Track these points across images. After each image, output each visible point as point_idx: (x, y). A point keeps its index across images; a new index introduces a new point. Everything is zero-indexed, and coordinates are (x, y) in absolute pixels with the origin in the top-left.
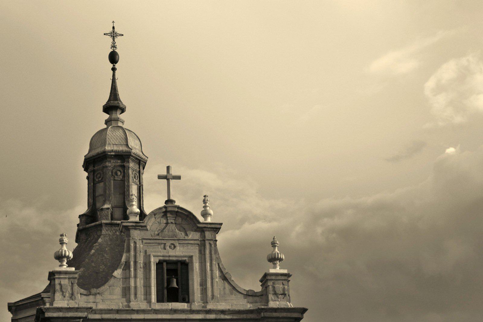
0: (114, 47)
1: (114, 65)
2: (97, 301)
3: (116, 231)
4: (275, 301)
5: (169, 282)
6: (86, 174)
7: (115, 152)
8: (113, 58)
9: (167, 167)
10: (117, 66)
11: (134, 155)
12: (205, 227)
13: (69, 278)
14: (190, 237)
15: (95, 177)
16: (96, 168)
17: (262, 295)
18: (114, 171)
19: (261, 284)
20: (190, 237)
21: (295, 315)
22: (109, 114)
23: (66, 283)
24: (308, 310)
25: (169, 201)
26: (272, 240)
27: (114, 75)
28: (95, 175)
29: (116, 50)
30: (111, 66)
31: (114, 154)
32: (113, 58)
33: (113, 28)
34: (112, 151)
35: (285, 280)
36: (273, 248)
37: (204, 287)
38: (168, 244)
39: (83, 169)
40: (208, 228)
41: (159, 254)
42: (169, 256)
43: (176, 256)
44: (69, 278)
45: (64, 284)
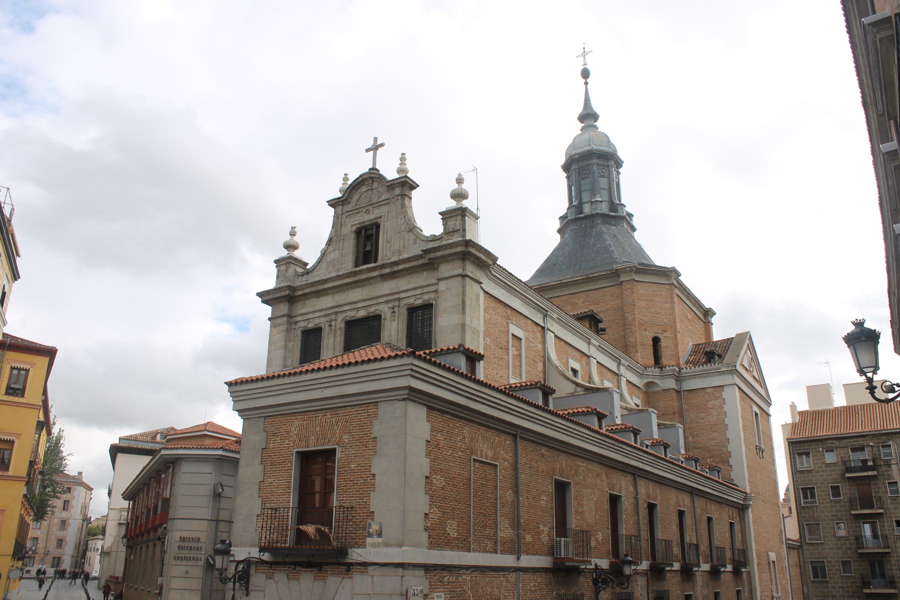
0: (585, 65)
1: (586, 80)
3: (582, 224)
5: (365, 246)
7: (579, 154)
8: (585, 74)
9: (375, 138)
10: (588, 80)
11: (596, 152)
12: (392, 185)
13: (286, 264)
14: (383, 198)
17: (442, 238)
18: (600, 171)
25: (373, 169)
27: (586, 88)
29: (587, 67)
30: (584, 81)
31: (577, 156)
32: (585, 74)
33: (584, 48)
34: (576, 154)
35: (458, 215)
36: (457, 185)
40: (395, 184)
42: (364, 222)
43: (369, 221)
44: (286, 264)
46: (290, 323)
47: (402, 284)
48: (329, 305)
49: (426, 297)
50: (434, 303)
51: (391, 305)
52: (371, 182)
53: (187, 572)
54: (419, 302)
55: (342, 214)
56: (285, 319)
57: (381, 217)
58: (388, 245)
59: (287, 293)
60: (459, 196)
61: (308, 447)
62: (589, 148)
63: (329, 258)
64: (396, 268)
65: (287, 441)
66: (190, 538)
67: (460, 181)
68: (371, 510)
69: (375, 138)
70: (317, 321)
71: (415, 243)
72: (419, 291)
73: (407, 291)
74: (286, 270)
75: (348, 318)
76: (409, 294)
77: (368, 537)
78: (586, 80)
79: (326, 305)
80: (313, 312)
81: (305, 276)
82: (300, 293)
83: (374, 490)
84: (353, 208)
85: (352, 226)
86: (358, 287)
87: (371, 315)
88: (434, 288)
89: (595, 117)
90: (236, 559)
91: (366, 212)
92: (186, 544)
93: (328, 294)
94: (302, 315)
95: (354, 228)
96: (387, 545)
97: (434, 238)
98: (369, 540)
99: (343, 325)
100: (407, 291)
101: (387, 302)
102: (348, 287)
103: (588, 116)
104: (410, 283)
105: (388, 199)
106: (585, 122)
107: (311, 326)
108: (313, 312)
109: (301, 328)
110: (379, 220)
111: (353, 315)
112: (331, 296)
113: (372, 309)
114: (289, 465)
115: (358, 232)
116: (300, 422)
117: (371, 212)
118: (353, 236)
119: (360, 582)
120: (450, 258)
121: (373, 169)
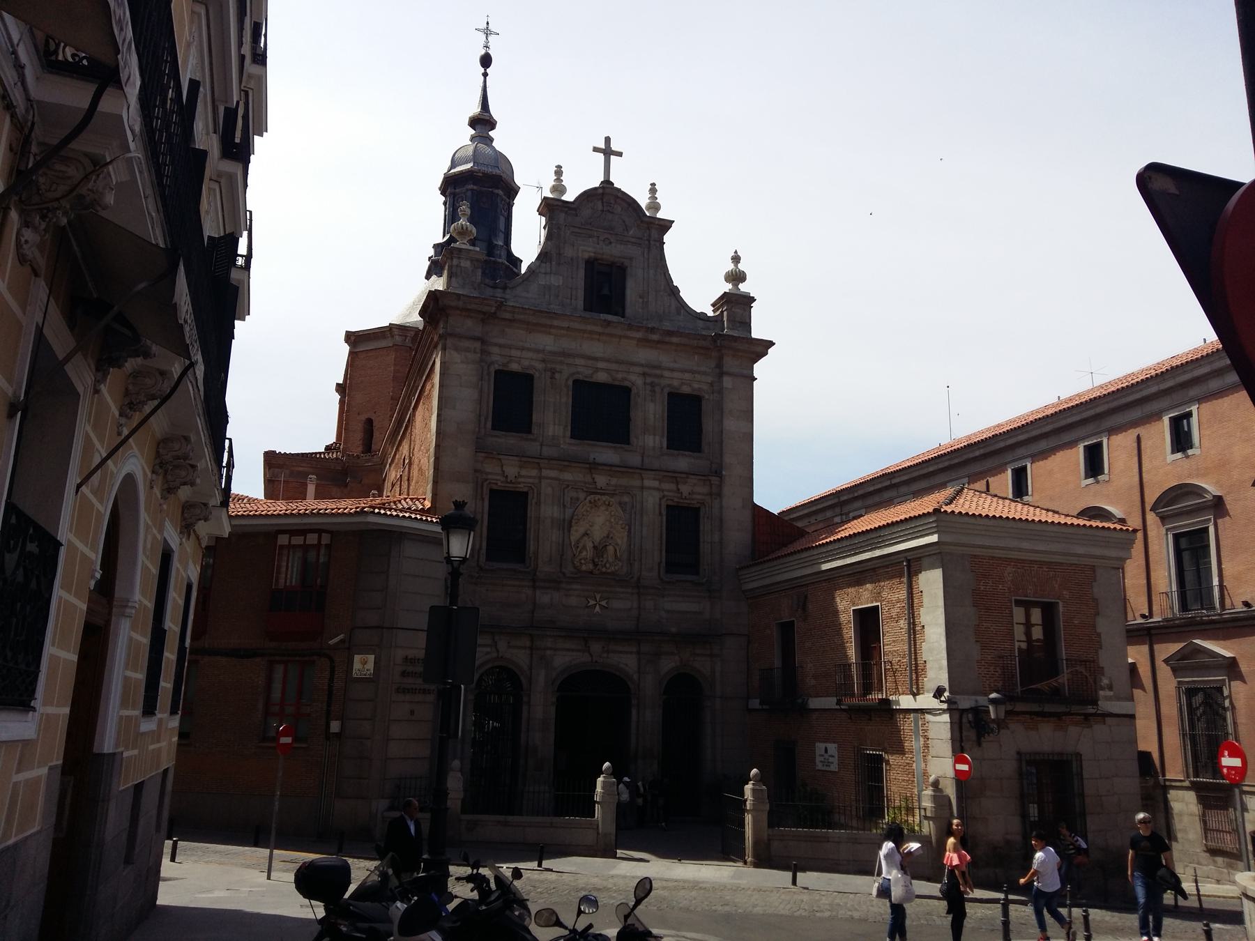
1: (485, 70)
2: (507, 297)
4: (733, 329)
6: (443, 198)
8: (486, 61)
9: (606, 138)
15: (455, 203)
16: (457, 190)
17: (716, 321)
19: (713, 309)
20: (631, 232)
21: (759, 349)
22: (475, 130)
23: (466, 266)
24: (774, 344)
25: (607, 183)
26: (733, 254)
27: (485, 82)
28: (456, 199)
30: (482, 70)
31: (481, 175)
32: (486, 61)
33: (488, 23)
37: (645, 300)
38: (602, 238)
39: (440, 192)
40: (654, 224)
41: (590, 249)
44: (472, 261)
45: (465, 268)
46: (483, 352)
47: (664, 359)
48: (548, 348)
49: (696, 386)
50: (707, 397)
51: (649, 380)
52: (612, 201)
53: (412, 712)
54: (686, 390)
55: (566, 225)
56: (478, 345)
57: (631, 259)
58: (641, 300)
59: (493, 310)
60: (736, 277)
61: (1027, 597)
62: (496, 171)
63: (542, 280)
64: (667, 339)
65: (1000, 586)
66: (419, 659)
67: (736, 259)
68: (1101, 666)
69: (606, 138)
70: (526, 363)
71: (679, 313)
72: (687, 376)
73: (672, 370)
74: (473, 271)
75: (580, 376)
76: (676, 375)
77: (1102, 690)
78: (485, 70)
79: (545, 346)
80: (523, 349)
81: (499, 290)
82: (508, 316)
83: (1101, 648)
84: (582, 225)
85: (583, 251)
86: (599, 340)
87: (617, 383)
88: (709, 379)
89: (491, 124)
90: (960, 707)
91: (604, 241)
92: (410, 669)
93: (550, 333)
94: (500, 346)
95: (586, 256)
96: (1118, 699)
97: (702, 317)
98: (1101, 693)
99: (570, 383)
100: (672, 370)
101: (644, 374)
102: (585, 335)
103: (483, 123)
104: (675, 362)
105: (639, 238)
106: (477, 127)
107: (514, 367)
108: (523, 349)
109: (497, 367)
110: (627, 263)
111: (584, 372)
112: (552, 337)
113: (620, 376)
114: (1007, 612)
115: (590, 264)
116: (1014, 569)
117: (613, 245)
118: (582, 266)
119: (1100, 731)
120: (740, 354)
121: (607, 183)
